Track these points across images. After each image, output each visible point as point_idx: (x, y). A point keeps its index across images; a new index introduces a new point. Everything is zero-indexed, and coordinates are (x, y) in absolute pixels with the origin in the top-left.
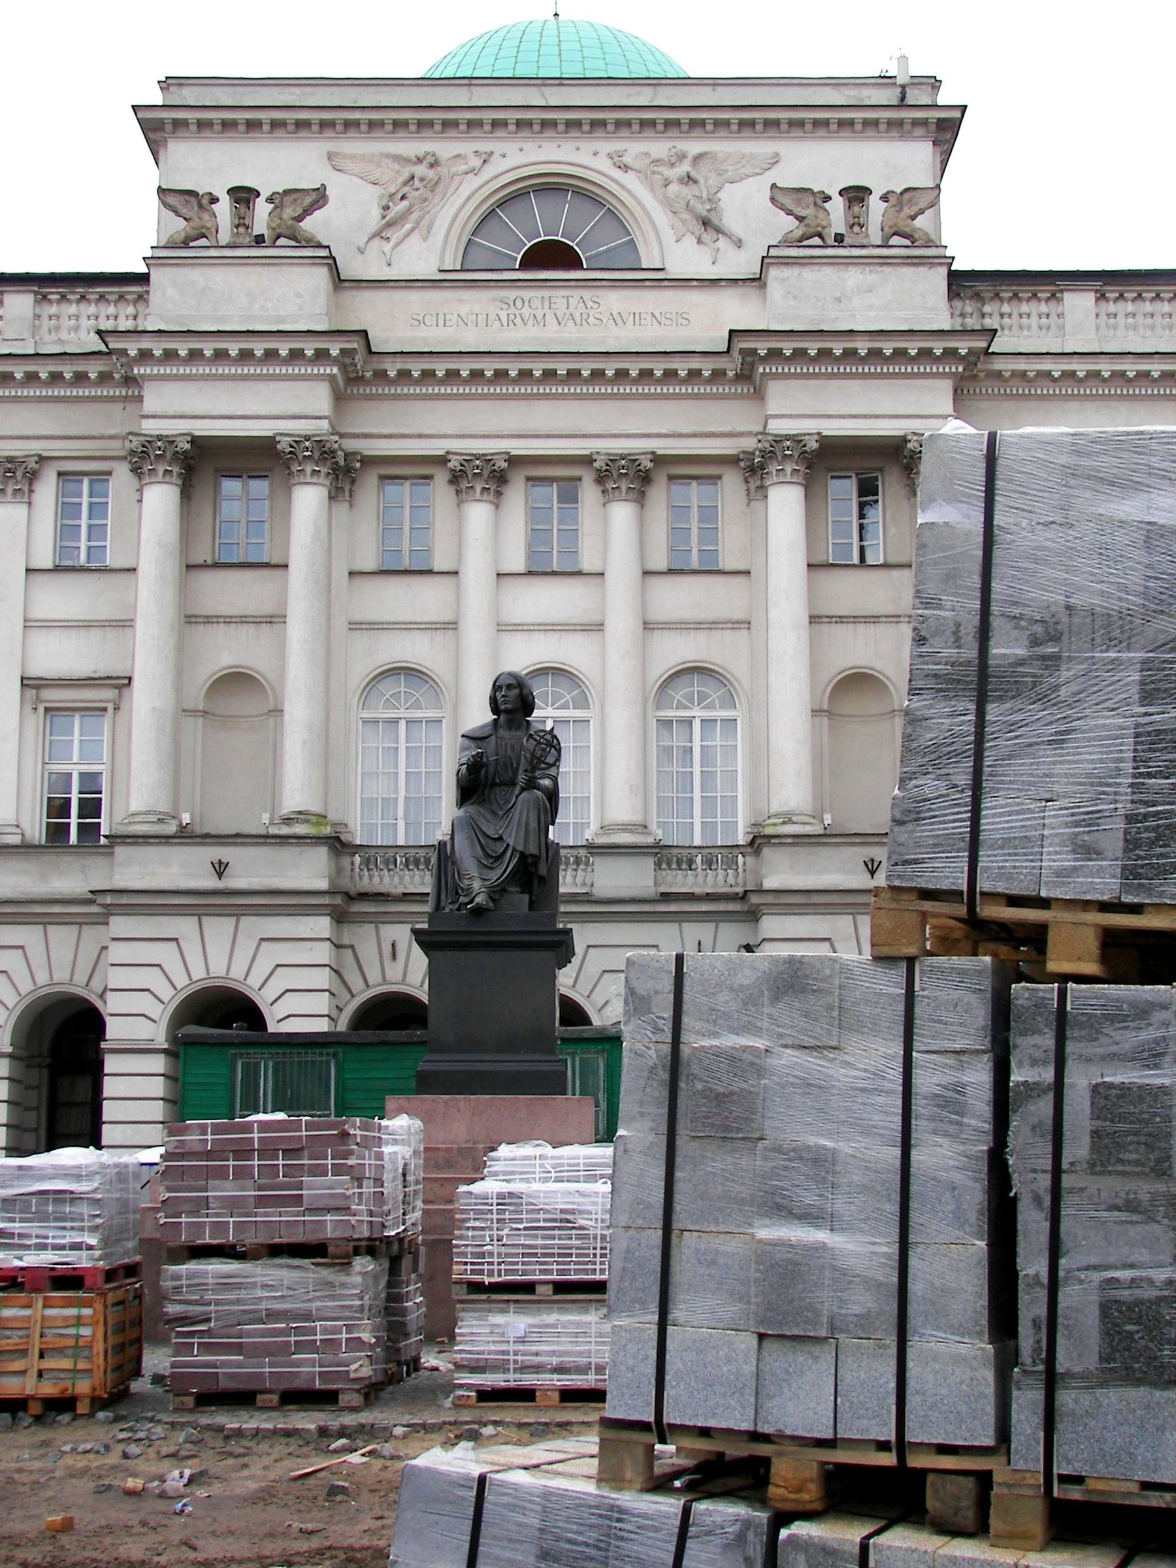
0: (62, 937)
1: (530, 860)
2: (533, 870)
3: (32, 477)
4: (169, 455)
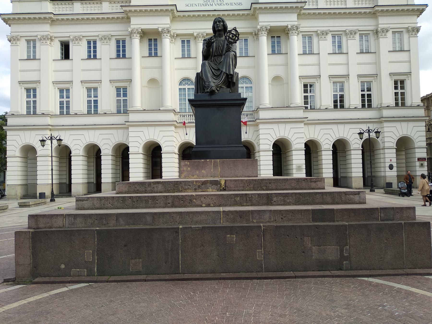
0: (120, 132)
1: (230, 77)
2: (230, 80)
3: (110, 39)
4: (137, 32)
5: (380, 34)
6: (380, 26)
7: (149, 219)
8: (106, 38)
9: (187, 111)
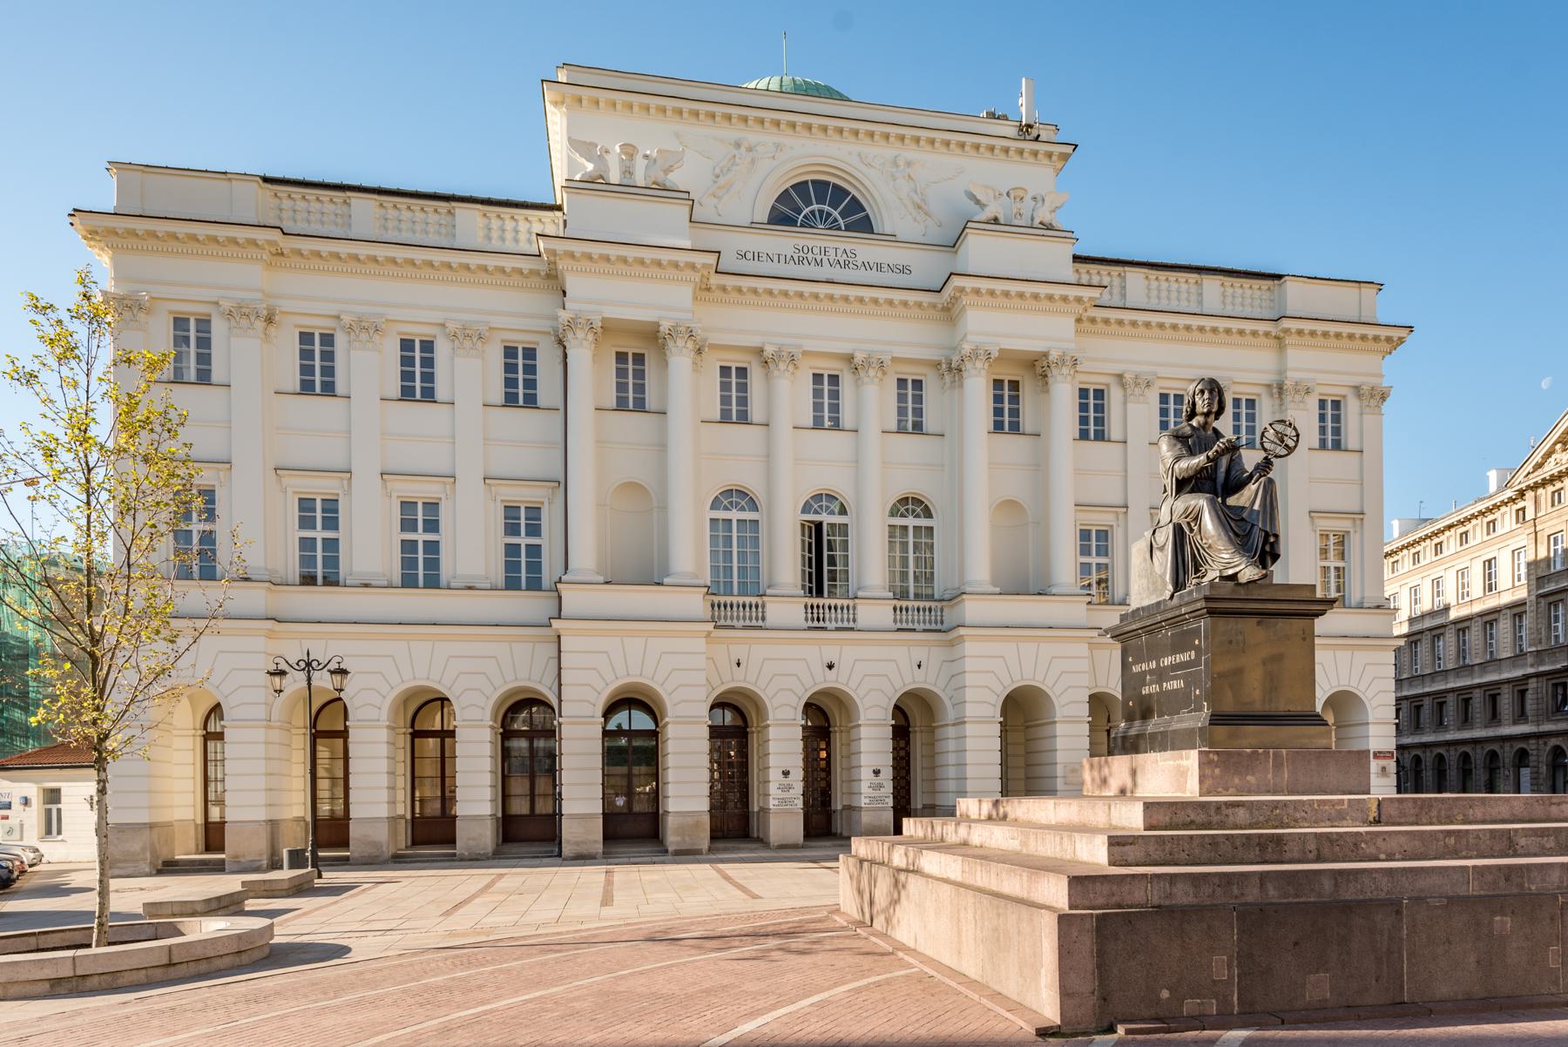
5: (1289, 398)
6: (1289, 374)
7: (1327, 885)
8: (469, 336)
9: (735, 591)
